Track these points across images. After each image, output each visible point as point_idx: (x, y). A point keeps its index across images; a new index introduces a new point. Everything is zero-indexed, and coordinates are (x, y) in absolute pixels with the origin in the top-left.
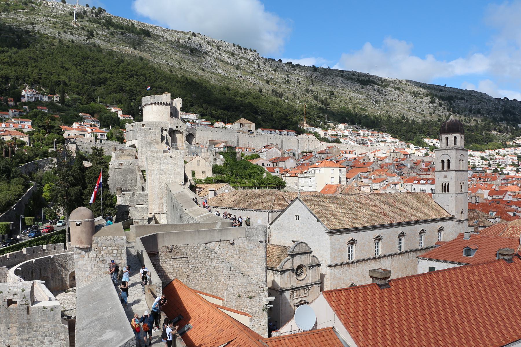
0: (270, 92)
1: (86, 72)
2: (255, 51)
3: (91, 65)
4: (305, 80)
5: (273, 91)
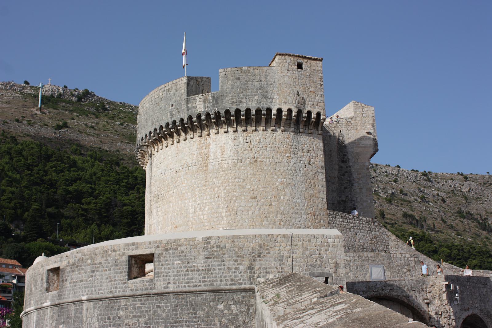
4: (451, 195)
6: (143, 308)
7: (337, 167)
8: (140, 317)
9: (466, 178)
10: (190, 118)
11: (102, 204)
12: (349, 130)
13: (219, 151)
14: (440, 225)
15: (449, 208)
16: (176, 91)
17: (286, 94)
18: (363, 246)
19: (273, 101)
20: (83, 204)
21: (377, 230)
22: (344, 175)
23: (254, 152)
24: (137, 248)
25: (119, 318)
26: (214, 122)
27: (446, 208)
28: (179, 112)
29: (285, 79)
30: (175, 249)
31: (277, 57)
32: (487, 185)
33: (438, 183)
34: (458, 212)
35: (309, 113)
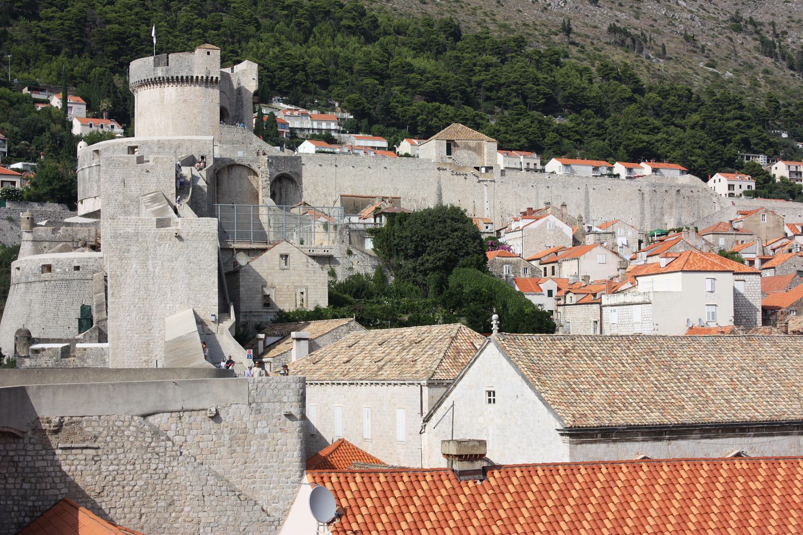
5: (613, 30)
10: (155, 78)
11: (72, 20)
14: (682, 46)
15: (716, 12)
20: (40, 19)
27: (711, 11)
34: (732, 19)
35: (212, 78)
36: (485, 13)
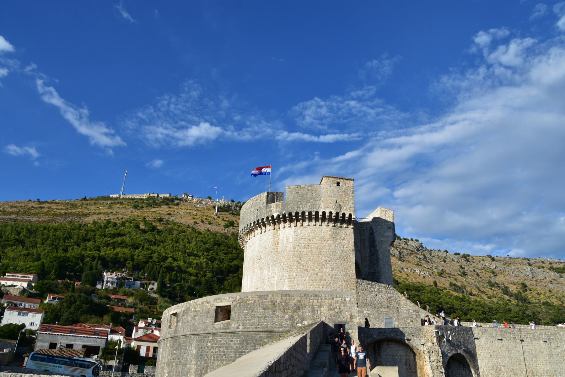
0: (447, 285)
1: (213, 260)
2: (417, 241)
3: (222, 252)
4: (483, 271)
5: (451, 284)
6: (222, 341)
7: (368, 250)
8: (220, 347)
9: (493, 259)
12: (377, 226)
13: (285, 239)
16: (260, 201)
17: (328, 202)
18: (381, 304)
19: (320, 207)
21: (391, 293)
22: (373, 255)
23: (307, 239)
24: (221, 302)
25: (208, 347)
26: (283, 221)
28: (261, 214)
29: (328, 193)
30: (244, 303)
31: (324, 178)
32: (508, 264)
33: (474, 263)
34: (488, 282)
35: (344, 214)
36: (404, 279)
